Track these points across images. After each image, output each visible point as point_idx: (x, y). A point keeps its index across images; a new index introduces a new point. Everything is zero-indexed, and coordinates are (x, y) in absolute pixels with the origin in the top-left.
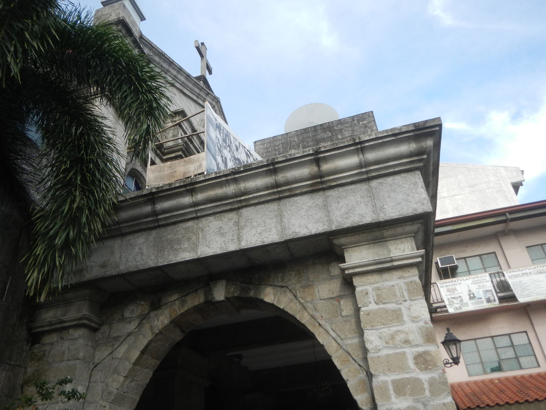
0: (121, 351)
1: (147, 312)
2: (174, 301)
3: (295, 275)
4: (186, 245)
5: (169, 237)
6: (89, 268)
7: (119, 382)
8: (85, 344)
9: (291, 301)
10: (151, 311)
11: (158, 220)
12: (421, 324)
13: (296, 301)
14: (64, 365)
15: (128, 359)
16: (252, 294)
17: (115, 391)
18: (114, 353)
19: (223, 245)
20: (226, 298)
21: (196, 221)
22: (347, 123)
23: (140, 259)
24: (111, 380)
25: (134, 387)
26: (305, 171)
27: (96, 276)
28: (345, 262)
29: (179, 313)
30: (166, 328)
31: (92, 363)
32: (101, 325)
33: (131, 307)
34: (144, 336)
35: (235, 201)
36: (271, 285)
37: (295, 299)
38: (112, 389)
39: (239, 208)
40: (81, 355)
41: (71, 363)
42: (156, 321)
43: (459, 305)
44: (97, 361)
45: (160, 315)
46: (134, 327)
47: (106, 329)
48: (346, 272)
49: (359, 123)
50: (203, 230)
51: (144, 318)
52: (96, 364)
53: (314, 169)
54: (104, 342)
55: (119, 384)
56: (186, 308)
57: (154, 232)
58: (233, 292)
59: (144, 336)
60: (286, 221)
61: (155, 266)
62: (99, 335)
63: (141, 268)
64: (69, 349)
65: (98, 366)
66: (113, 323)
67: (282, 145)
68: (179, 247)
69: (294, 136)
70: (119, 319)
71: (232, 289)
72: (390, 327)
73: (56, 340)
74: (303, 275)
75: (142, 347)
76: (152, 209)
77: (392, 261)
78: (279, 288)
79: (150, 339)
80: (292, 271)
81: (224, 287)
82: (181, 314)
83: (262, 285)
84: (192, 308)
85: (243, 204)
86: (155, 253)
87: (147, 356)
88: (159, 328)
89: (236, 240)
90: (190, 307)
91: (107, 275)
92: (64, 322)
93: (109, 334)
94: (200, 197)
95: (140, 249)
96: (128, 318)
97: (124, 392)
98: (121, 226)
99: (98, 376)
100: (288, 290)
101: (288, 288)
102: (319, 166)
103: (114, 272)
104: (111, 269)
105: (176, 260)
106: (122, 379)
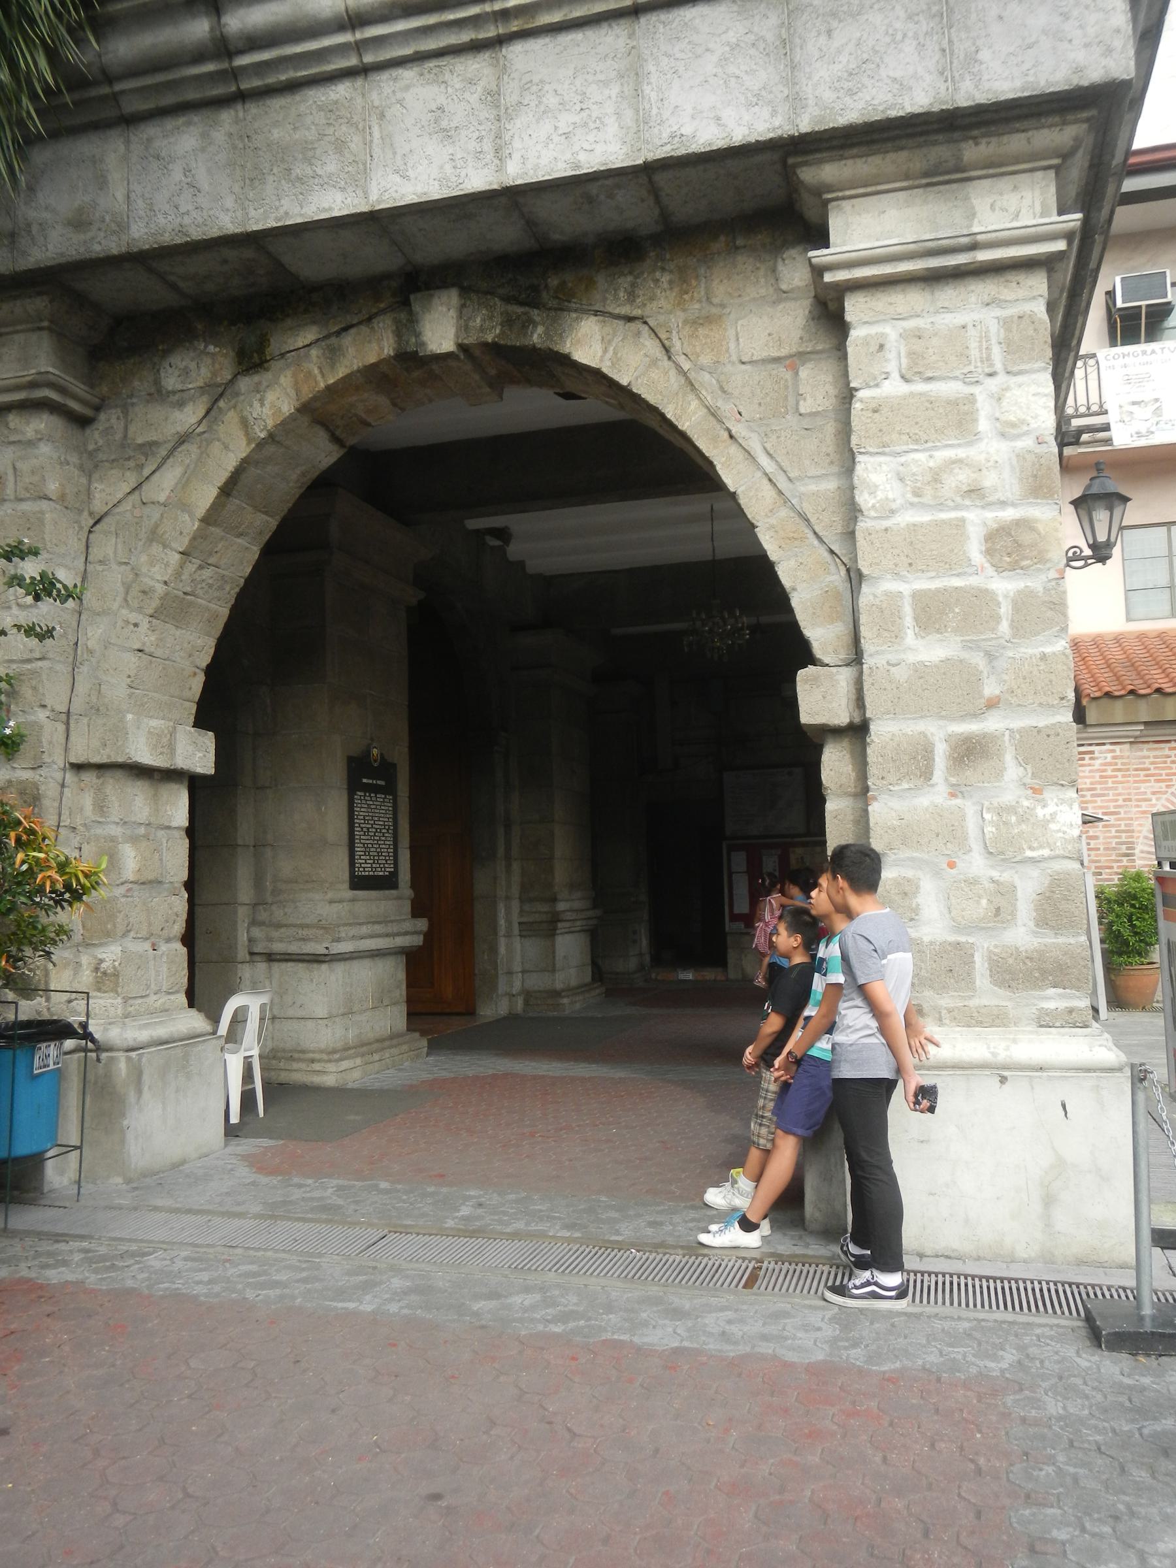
0: (166, 482)
1: (229, 377)
2: (304, 347)
3: (671, 282)
4: (330, 166)
5: (276, 134)
6: (35, 229)
7: (167, 565)
8: (59, 458)
9: (654, 362)
10: (239, 373)
11: (235, 74)
12: (1027, 443)
13: (666, 363)
14: (9, 511)
15: (185, 507)
16: (537, 337)
17: (160, 589)
18: (145, 487)
19: (448, 168)
20: (461, 347)
21: (359, 82)
23: (190, 207)
24: (144, 558)
25: (210, 581)
27: (62, 255)
28: (828, 247)
29: (322, 385)
30: (286, 425)
31: (86, 513)
32: (98, 409)
34: (226, 447)
35: (487, 13)
36: (596, 313)
37: (666, 358)
38: (151, 583)
39: (500, 41)
40: (52, 487)
41: (26, 506)
42: (256, 404)
43: (1148, 424)
44: (99, 506)
45: (268, 386)
46: (194, 420)
47: (114, 421)
48: (828, 278)
50: (382, 116)
51: (221, 395)
52: (97, 517)
54: (113, 457)
55: (170, 571)
56: (341, 372)
57: (226, 116)
58: (482, 329)
59: (226, 447)
60: (653, 96)
61: (238, 230)
62: (95, 436)
63: (196, 234)
64: (15, 468)
65: (106, 520)
66: (133, 404)
68: (311, 173)
70: (150, 394)
71: (478, 320)
72: (935, 448)
74: (694, 283)
75: (222, 476)
76: (212, 29)
77: (974, 247)
78: (621, 323)
79: (244, 455)
80: (663, 269)
81: (453, 313)
82: (328, 388)
83: (569, 310)
84: (359, 371)
85: (515, 26)
86: (237, 188)
87: (238, 502)
88: (265, 426)
89: (489, 157)
90: (355, 367)
91: (94, 255)
93: (125, 436)
95: (187, 171)
96: (174, 392)
97: (185, 593)
98: (118, 87)
99: (106, 546)
100: (645, 330)
101: (645, 323)
103: (114, 246)
104: (102, 234)
105: (301, 215)
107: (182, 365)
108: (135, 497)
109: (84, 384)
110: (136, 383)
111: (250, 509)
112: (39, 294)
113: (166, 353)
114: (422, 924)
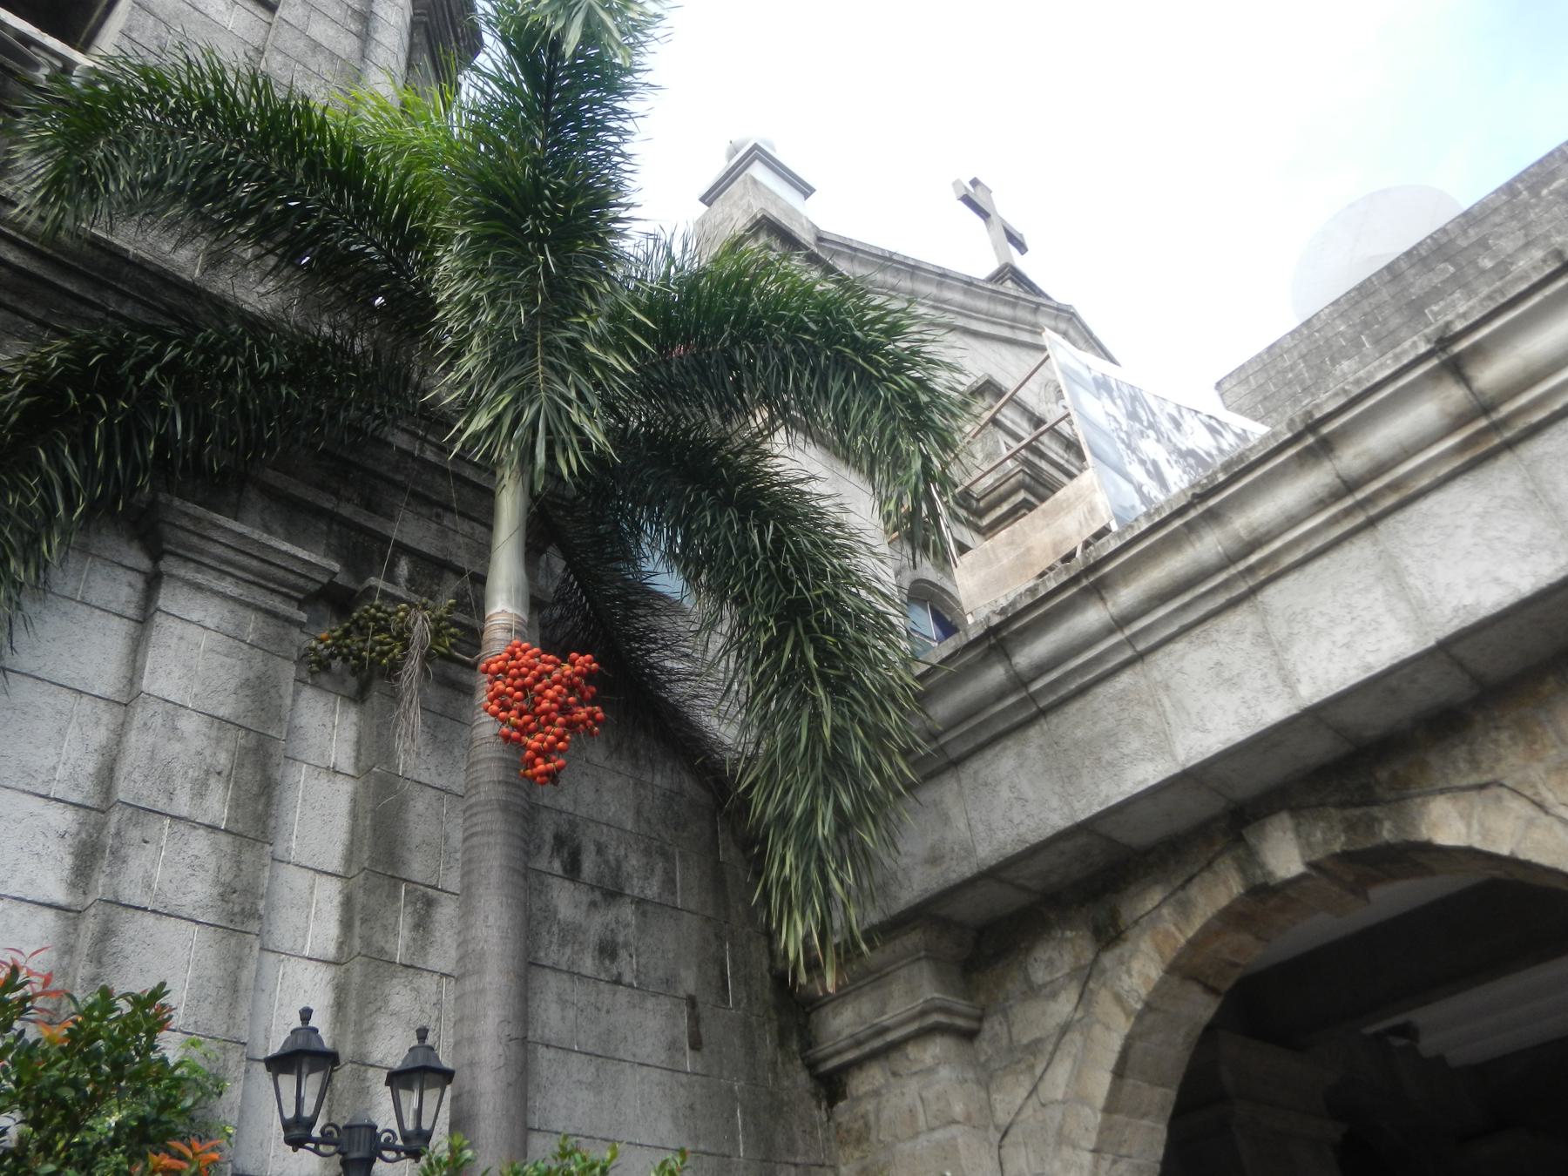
0: (1059, 1078)
1: (1091, 957)
2: (1155, 908)
3: (1512, 738)
4: (1135, 743)
5: (1079, 733)
6: (900, 875)
7: (1081, 1167)
9: (1530, 823)
11: (1033, 698)
13: (1545, 820)
14: (925, 1143)
15: (1083, 1100)
16: (1387, 833)
18: (1041, 1088)
19: (1243, 711)
20: (1311, 865)
21: (1138, 667)
22: (1496, 210)
23: (1023, 817)
24: (1057, 1165)
26: (1426, 412)
27: (926, 890)
29: (1182, 941)
30: (1159, 990)
31: (992, 1129)
32: (980, 1019)
33: (1043, 953)
34: (1107, 1028)
35: (1234, 575)
36: (1442, 791)
37: (1542, 815)
39: (1253, 591)
40: (958, 1109)
41: (939, 1135)
42: (1125, 977)
44: (1002, 1118)
45: (1131, 956)
47: (997, 1027)
49: (1537, 194)
50: (1167, 687)
51: (1089, 977)
52: (1003, 1129)
53: (1453, 395)
54: (1004, 1064)
56: (1197, 923)
57: (1033, 732)
58: (1326, 842)
59: (1107, 1028)
60: (1420, 583)
61: (1069, 823)
62: (984, 1046)
63: (1033, 838)
64: (922, 1099)
65: (1012, 1132)
66: (1011, 1007)
67: (1305, 361)
68: (1117, 755)
69: (1334, 319)
70: (1024, 993)
71: (1319, 835)
73: (882, 1081)
74: (1538, 730)
75: (1111, 1059)
76: (1007, 672)
78: (1473, 794)
80: (1497, 728)
81: (1290, 835)
82: (1191, 943)
83: (1411, 797)
85: (1262, 575)
86: (1058, 789)
89: (1279, 688)
90: (1209, 914)
91: (952, 883)
92: (885, 1030)
93: (1011, 1039)
94: (1126, 596)
95: (1012, 788)
96: (1045, 985)
98: (942, 741)
100: (1505, 793)
101: (1502, 785)
102: (1465, 380)
103: (967, 870)
104: (954, 862)
105: (1121, 794)
106: (1087, 1158)
107: (1045, 957)
108: (1034, 1100)
109: (964, 999)
110: (1009, 986)
111: (1146, 1085)
112: (913, 929)
113: (1028, 950)
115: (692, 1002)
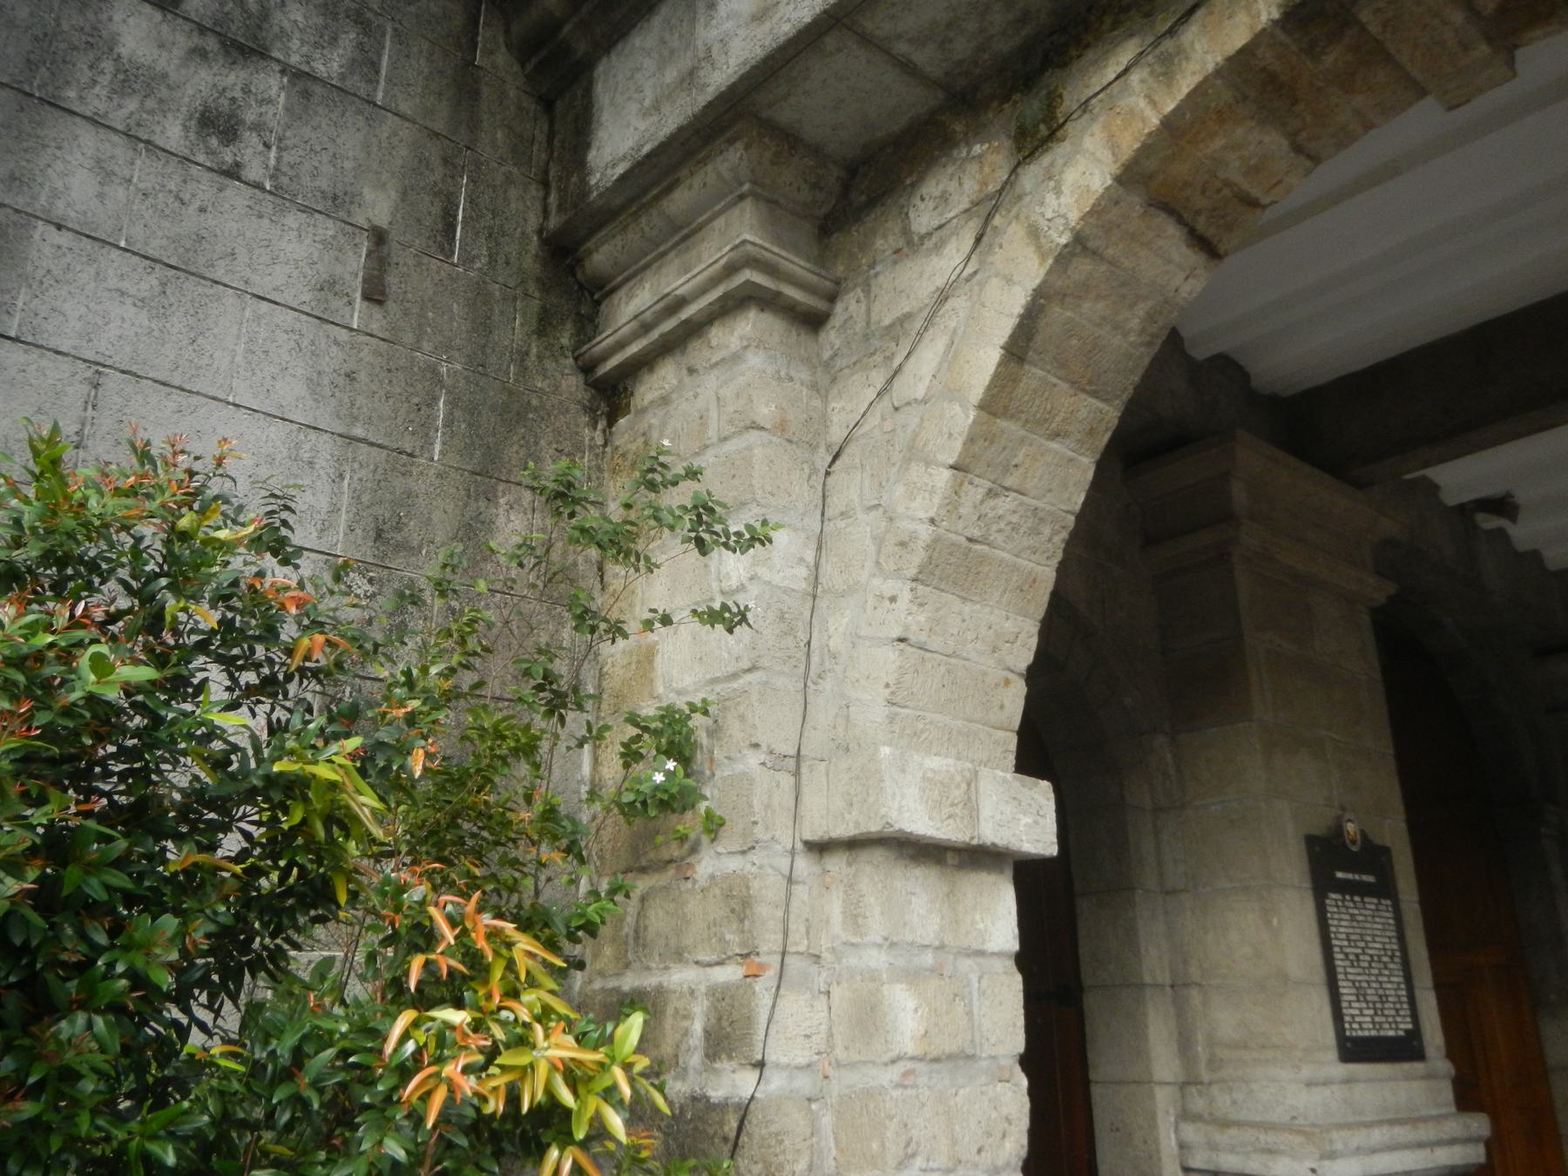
8: (778, 372)
10: (1019, 164)
15: (953, 393)
17: (925, 532)
24: (900, 490)
25: (1015, 519)
29: (1155, 121)
31: (822, 450)
32: (832, 298)
33: (932, 187)
34: (1009, 280)
38: (912, 526)
41: (729, 447)
42: (1050, 198)
44: (837, 434)
45: (1065, 164)
46: (958, 259)
47: (853, 306)
51: (995, 208)
54: (854, 359)
55: (937, 500)
56: (1186, 84)
62: (831, 336)
65: (848, 451)
66: (876, 275)
70: (897, 251)
73: (675, 382)
75: (1003, 328)
79: (1038, 281)
82: (1168, 123)
84: (1218, 72)
87: (1040, 373)
88: (1066, 224)
90: (1210, 67)
91: (782, 39)
92: (681, 302)
93: (868, 323)
96: (929, 234)
97: (970, 540)
99: (850, 487)
106: (943, 477)
107: (937, 193)
108: (885, 402)
109: (808, 259)
110: (879, 243)
111: (1064, 386)
112: (731, 141)
114: (1479, 1124)
115: (379, 237)
